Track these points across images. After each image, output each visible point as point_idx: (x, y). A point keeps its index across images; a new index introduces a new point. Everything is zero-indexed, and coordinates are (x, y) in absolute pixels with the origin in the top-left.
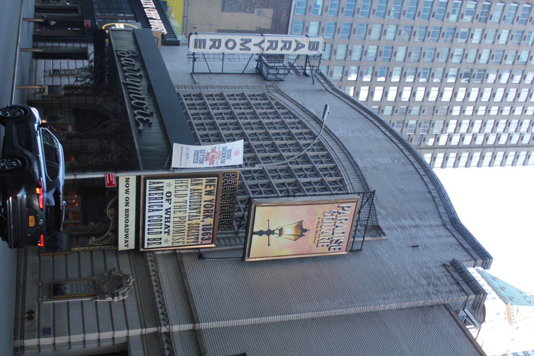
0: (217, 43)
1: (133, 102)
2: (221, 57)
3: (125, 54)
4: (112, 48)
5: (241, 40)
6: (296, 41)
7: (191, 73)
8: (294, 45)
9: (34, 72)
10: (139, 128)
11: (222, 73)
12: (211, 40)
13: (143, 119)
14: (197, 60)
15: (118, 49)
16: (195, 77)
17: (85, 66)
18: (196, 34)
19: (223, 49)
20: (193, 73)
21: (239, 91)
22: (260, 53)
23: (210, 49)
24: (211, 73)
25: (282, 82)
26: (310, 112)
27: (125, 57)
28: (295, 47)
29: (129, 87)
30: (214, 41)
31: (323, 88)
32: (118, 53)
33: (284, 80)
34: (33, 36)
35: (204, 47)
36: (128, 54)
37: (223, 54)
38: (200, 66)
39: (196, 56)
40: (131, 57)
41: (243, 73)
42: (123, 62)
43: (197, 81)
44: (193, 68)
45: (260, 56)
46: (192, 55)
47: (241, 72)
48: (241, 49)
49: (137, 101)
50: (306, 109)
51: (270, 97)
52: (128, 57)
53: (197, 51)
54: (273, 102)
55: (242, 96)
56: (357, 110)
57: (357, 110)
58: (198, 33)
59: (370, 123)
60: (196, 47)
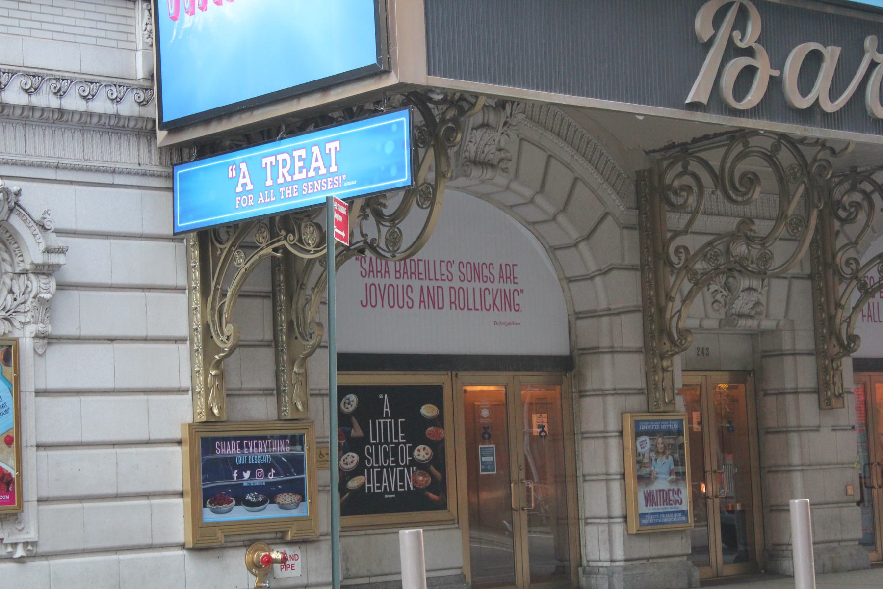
27: (775, 83)
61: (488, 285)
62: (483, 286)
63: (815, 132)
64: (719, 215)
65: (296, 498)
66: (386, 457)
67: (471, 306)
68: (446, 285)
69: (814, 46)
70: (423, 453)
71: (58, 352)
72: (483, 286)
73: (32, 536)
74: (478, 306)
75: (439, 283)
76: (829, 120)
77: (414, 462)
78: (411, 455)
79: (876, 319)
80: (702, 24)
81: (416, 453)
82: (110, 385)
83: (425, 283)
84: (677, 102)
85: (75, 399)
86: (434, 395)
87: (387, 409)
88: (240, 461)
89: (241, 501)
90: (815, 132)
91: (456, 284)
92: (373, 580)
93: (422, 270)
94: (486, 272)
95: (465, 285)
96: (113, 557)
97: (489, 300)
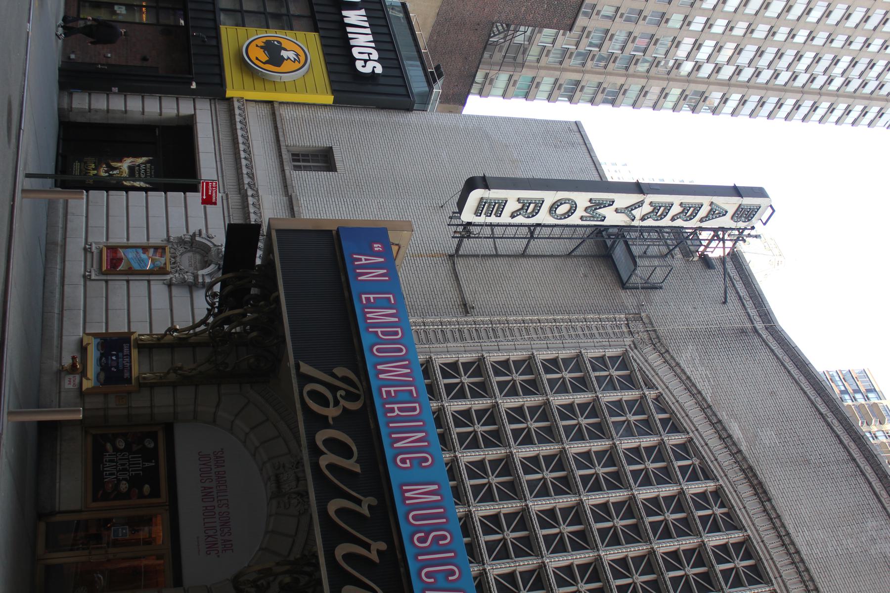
3: (326, 404)
6: (712, 203)
7: (451, 256)
8: (703, 213)
9: (59, 260)
16: (460, 264)
17: (191, 233)
25: (657, 295)
26: (734, 444)
28: (704, 215)
30: (525, 205)
31: (749, 325)
33: (661, 288)
34: (60, 70)
41: (569, 255)
42: (323, 462)
50: (724, 429)
51: (640, 369)
54: (651, 394)
56: (828, 425)
57: (828, 425)
59: (861, 480)
60: (478, 213)
65: (102, 381)
66: (122, 465)
67: (206, 520)
69: (354, 449)
70: (124, 486)
71: (165, 289)
73: (93, 277)
74: (207, 525)
76: (316, 467)
77: (119, 481)
78: (124, 479)
80: (340, 371)
81: (124, 482)
82: (153, 307)
85: (147, 295)
86: (155, 493)
87: (147, 464)
88: (120, 354)
89: (102, 355)
92: (58, 457)
93: (222, 488)
94: (226, 530)
96: (82, 308)
97: (211, 533)
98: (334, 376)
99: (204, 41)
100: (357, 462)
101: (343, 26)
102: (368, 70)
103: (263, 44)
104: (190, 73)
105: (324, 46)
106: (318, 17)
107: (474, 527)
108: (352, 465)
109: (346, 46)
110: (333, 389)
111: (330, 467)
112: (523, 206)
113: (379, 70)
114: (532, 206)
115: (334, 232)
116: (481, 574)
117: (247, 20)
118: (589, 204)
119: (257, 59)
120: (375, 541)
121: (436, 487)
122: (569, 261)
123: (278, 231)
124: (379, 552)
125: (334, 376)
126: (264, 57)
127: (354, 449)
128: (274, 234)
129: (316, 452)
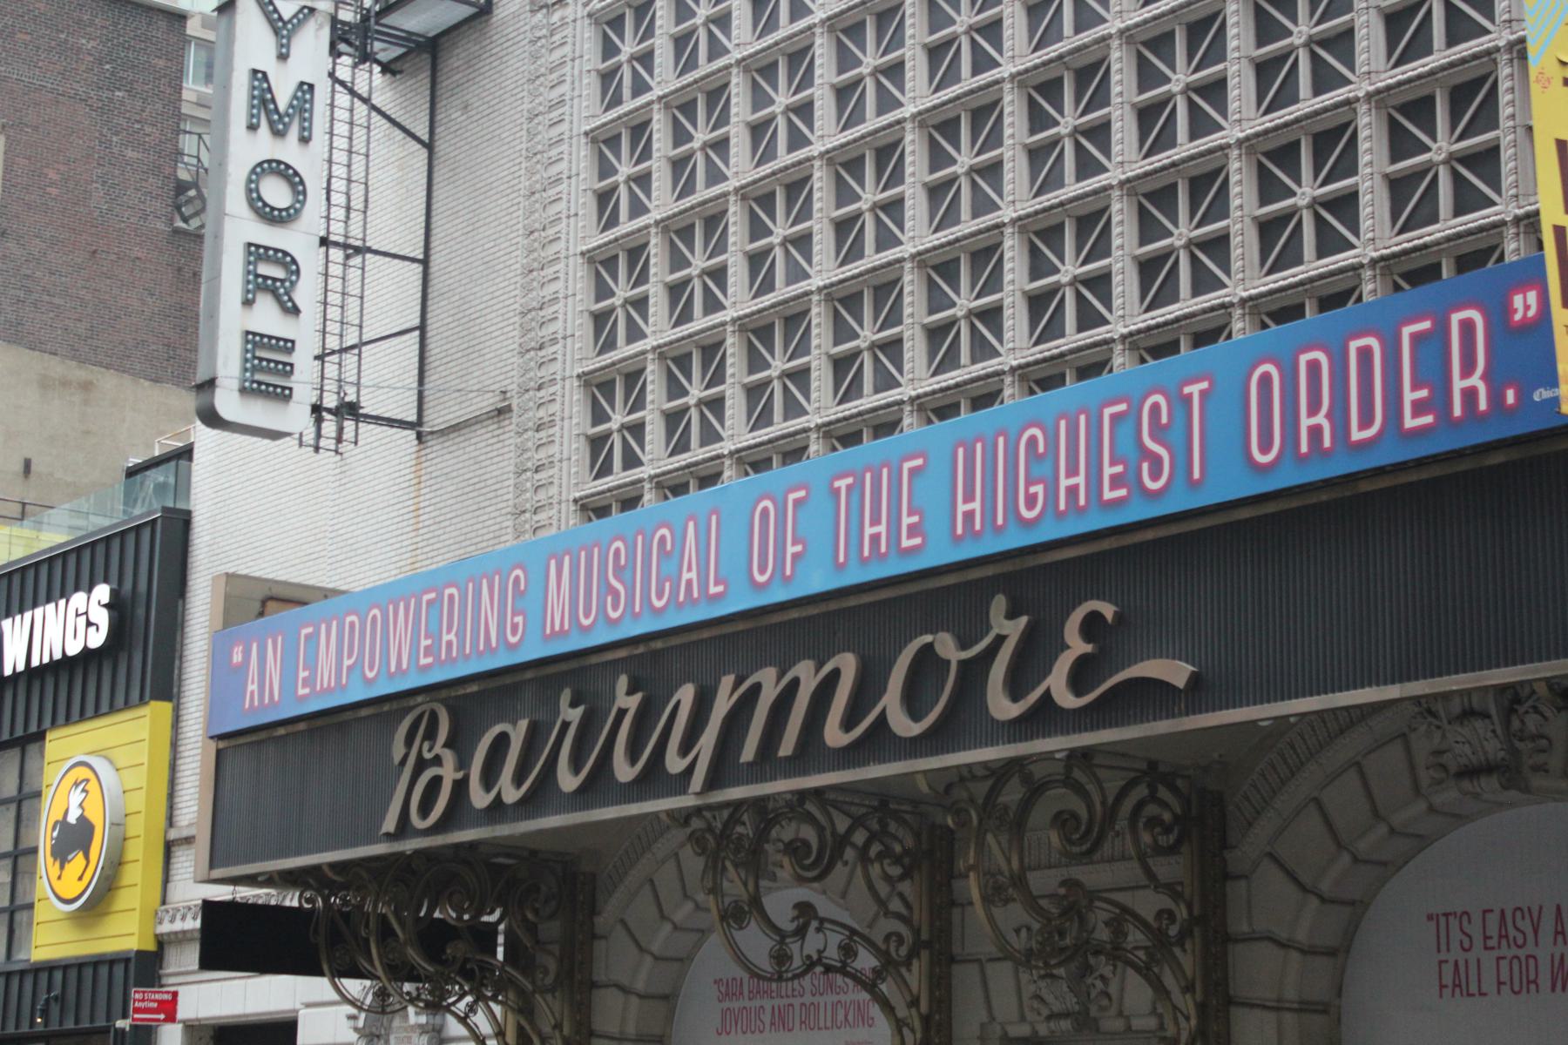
0: (264, 269)
1: (904, 726)
2: (336, 254)
3: (436, 782)
4: (335, 866)
5: (252, 128)
7: (420, 437)
10: (1180, 681)
11: (425, 262)
12: (248, 303)
13: (1082, 664)
14: (351, 398)
15: (389, 825)
16: (436, 418)
18: (210, 384)
19: (298, 241)
20: (416, 425)
21: (579, 160)
22: (326, 33)
23: (295, 311)
24: (422, 328)
27: (461, 787)
29: (748, 753)
30: (256, 287)
32: (417, 822)
35: (288, 345)
36: (437, 761)
37: (324, 242)
38: (385, 380)
39: (330, 401)
40: (460, 743)
41: (429, 146)
42: (511, 795)
43: (488, 402)
44: (391, 422)
45: (340, 36)
46: (319, 421)
47: (424, 153)
48: (305, 140)
49: (891, 701)
52: (463, 763)
53: (304, 394)
55: (618, 140)
58: (201, 376)
60: (283, 395)
61: (843, 997)
62: (835, 998)
63: (503, 830)
64: (1050, 867)
67: (822, 1024)
68: (797, 1002)
69: (497, 729)
72: (835, 998)
75: (791, 1001)
79: (1473, 988)
83: (777, 1002)
84: (371, 840)
90: (503, 830)
91: (808, 999)
95: (816, 999)
97: (841, 1016)
98: (403, 762)
99: (56, 998)
100: (514, 723)
101: (32, 674)
102: (102, 617)
103: (58, 864)
104: (105, 1031)
105: (68, 721)
106: (19, 732)
107: (845, 419)
108: (518, 733)
109: (64, 666)
110: (421, 765)
111: (518, 780)
112: (266, 289)
113: (102, 592)
114: (264, 269)
115: (222, 745)
116: (1134, 347)
117: (27, 901)
118: (264, 128)
119: (80, 878)
120: (613, 698)
121: (553, 563)
122: (441, 146)
123: (212, 866)
124: (631, 692)
125: (403, 762)
126: (78, 861)
127: (497, 729)
128: (218, 873)
129: (497, 809)
